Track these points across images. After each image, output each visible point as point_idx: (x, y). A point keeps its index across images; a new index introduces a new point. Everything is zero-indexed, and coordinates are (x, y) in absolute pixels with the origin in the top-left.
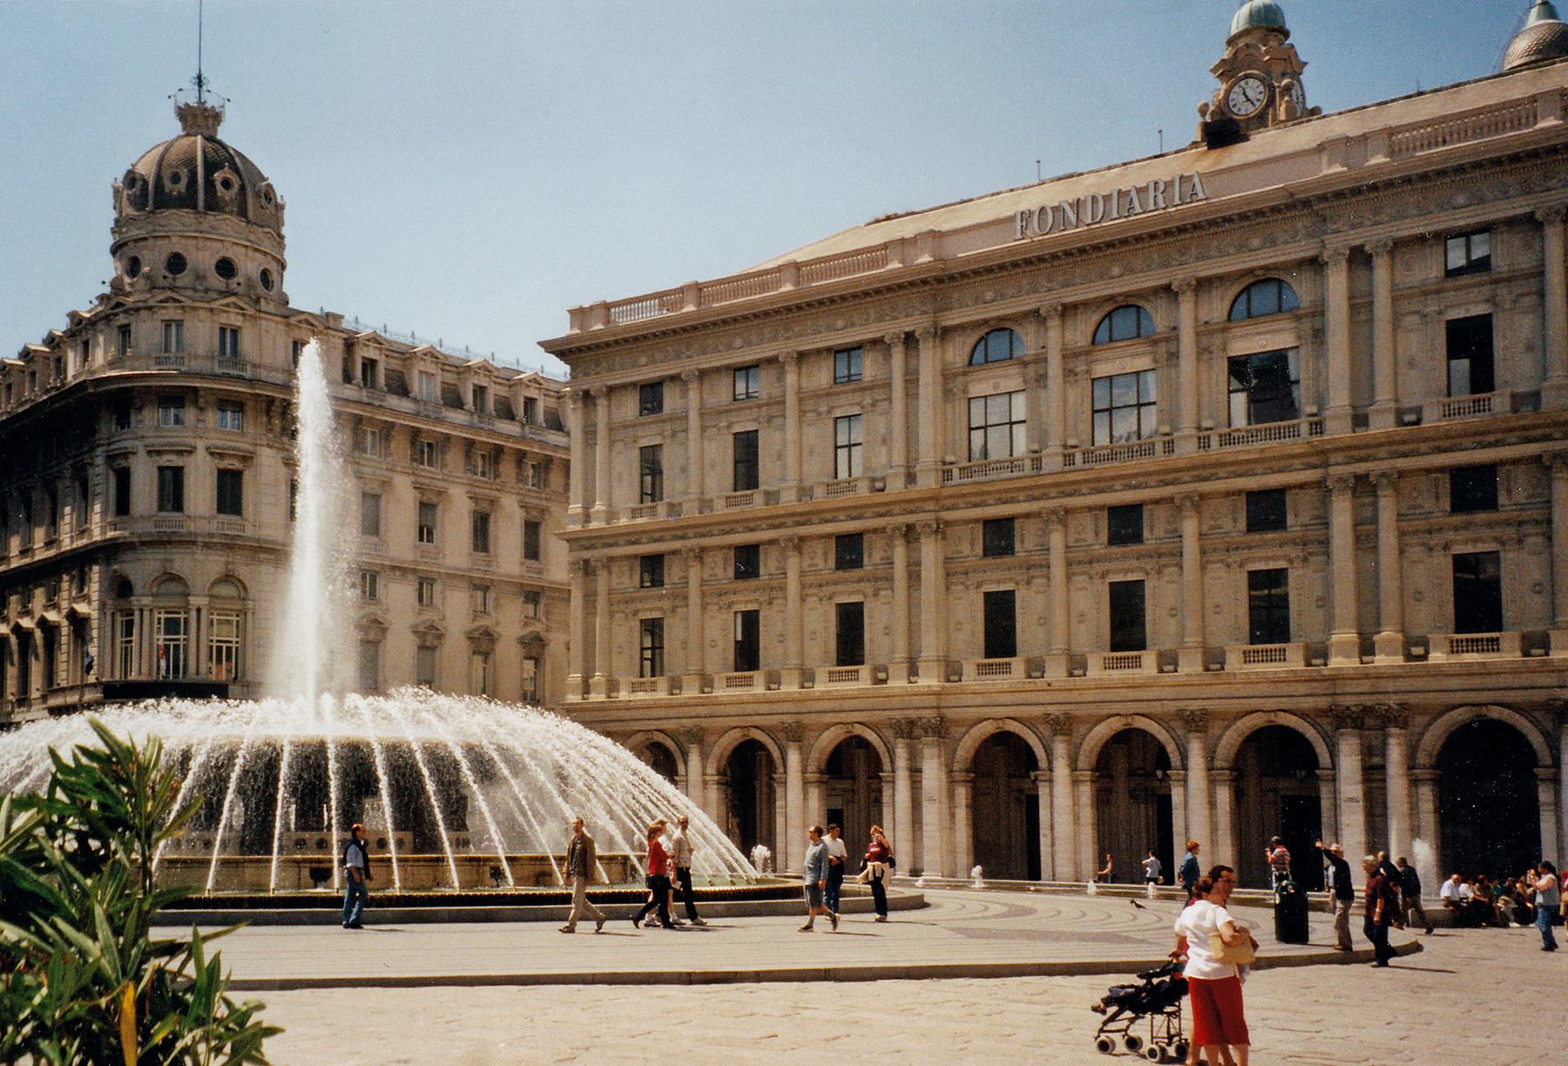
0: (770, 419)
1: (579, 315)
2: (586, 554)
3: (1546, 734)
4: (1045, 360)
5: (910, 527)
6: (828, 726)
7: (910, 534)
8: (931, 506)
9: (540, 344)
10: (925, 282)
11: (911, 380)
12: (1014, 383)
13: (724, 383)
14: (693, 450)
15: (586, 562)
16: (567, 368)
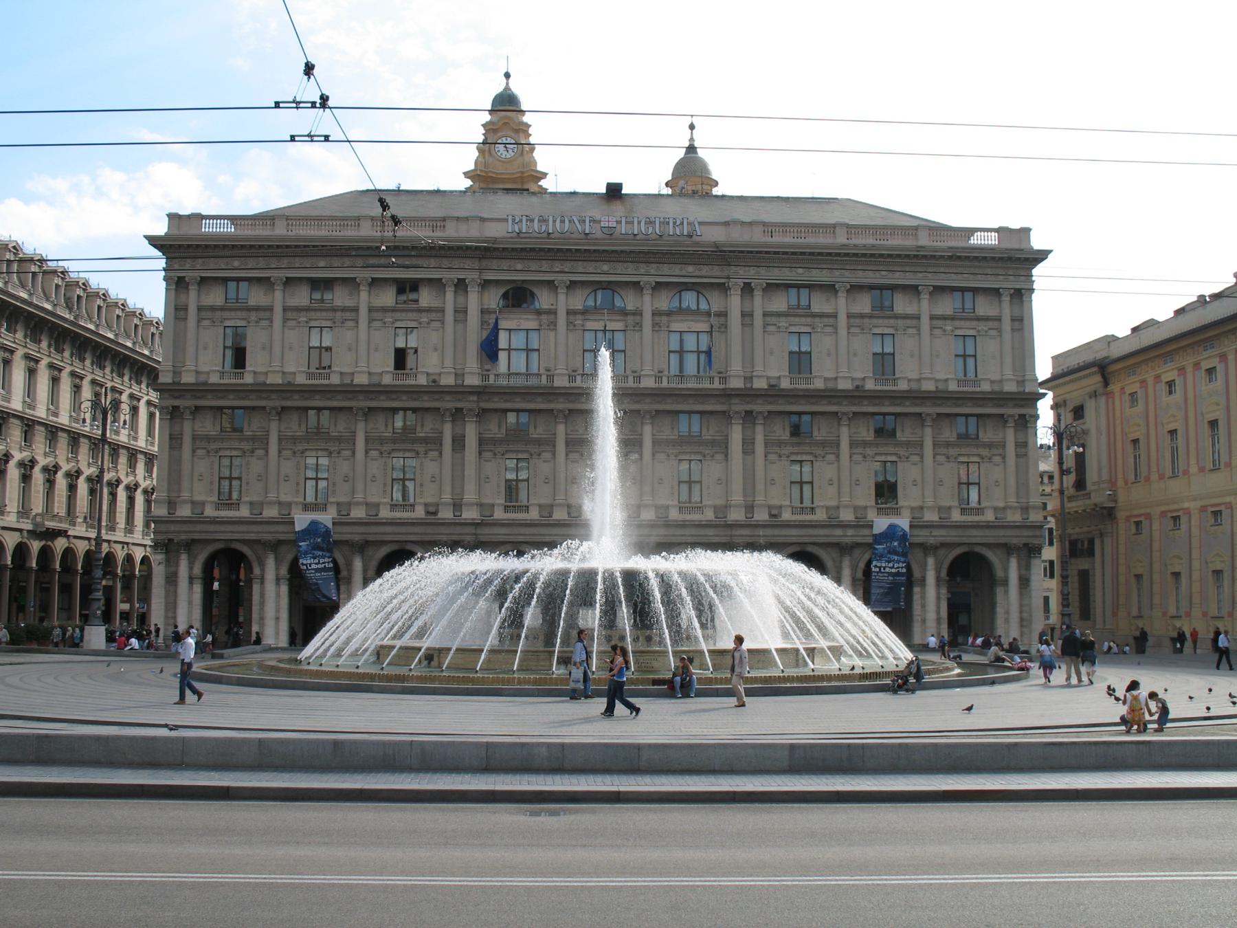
1: (172, 217)
2: (176, 403)
3: (834, 561)
4: (555, 313)
5: (459, 410)
6: (384, 543)
8: (475, 398)
9: (146, 237)
11: (461, 312)
12: (532, 324)
15: (175, 408)
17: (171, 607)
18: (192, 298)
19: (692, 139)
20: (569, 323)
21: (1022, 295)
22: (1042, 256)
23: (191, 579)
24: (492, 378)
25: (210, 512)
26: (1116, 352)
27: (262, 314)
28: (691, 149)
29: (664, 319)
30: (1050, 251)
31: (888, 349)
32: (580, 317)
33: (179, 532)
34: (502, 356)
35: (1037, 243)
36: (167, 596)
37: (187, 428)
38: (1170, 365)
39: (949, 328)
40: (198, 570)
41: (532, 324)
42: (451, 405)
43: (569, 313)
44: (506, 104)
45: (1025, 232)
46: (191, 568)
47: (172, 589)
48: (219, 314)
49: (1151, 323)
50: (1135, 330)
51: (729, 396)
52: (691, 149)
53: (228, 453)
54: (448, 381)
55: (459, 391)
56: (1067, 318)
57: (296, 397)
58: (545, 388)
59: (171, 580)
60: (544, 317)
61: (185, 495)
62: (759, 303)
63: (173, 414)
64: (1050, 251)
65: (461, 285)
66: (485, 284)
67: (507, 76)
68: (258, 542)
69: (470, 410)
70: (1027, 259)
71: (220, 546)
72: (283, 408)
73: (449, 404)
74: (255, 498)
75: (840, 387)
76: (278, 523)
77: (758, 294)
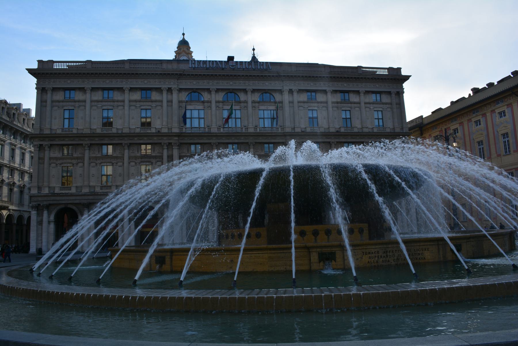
0: (118, 106)
1: (40, 62)
2: (41, 143)
5: (170, 144)
7: (170, 145)
8: (177, 138)
9: (27, 69)
10: (176, 74)
11: (170, 102)
13: (100, 92)
14: (88, 112)
15: (41, 145)
16: (36, 80)
17: (39, 236)
18: (49, 97)
19: (254, 54)
20: (217, 107)
21: (400, 93)
22: (407, 78)
23: (49, 222)
24: (184, 129)
25: (57, 191)
26: (425, 122)
27: (81, 104)
28: (254, 58)
29: (257, 104)
30: (410, 76)
31: (348, 116)
32: (221, 104)
33: (43, 201)
34: (188, 121)
35: (404, 73)
36: (37, 231)
37: (47, 154)
38: (454, 123)
39: (372, 107)
40: (52, 218)
41: (201, 107)
42: (167, 141)
43: (217, 102)
45: (399, 69)
46: (49, 217)
47: (40, 227)
48: (61, 103)
49: (440, 109)
50: (433, 113)
51: (285, 136)
52: (254, 58)
53: (66, 165)
54: (165, 130)
55: (170, 135)
56: (419, 103)
57: (97, 139)
58: (208, 133)
59: (40, 223)
60: (206, 104)
61: (46, 184)
62: (297, 98)
63: (40, 148)
64: (410, 76)
65: (170, 90)
66: (180, 90)
67: (183, 34)
68: (80, 204)
69: (175, 143)
70: (401, 79)
71: (63, 206)
72: (91, 144)
73: (165, 141)
74: (79, 184)
75: (331, 131)
76: (88, 195)
77: (295, 94)
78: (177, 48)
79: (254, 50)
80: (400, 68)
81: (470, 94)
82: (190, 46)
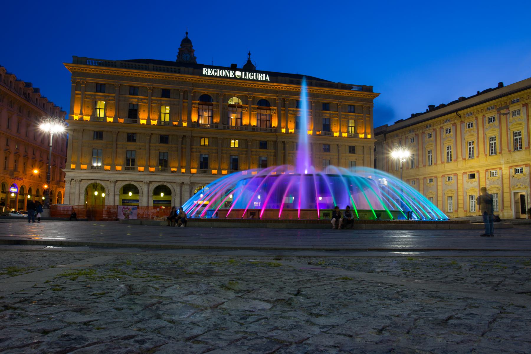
19: (249, 58)
28: (249, 62)
31: (327, 123)
44: (186, 42)
52: (249, 62)
67: (187, 33)
71: (93, 181)
78: (181, 45)
79: (249, 54)
80: (372, 87)
81: (427, 110)
82: (193, 45)
